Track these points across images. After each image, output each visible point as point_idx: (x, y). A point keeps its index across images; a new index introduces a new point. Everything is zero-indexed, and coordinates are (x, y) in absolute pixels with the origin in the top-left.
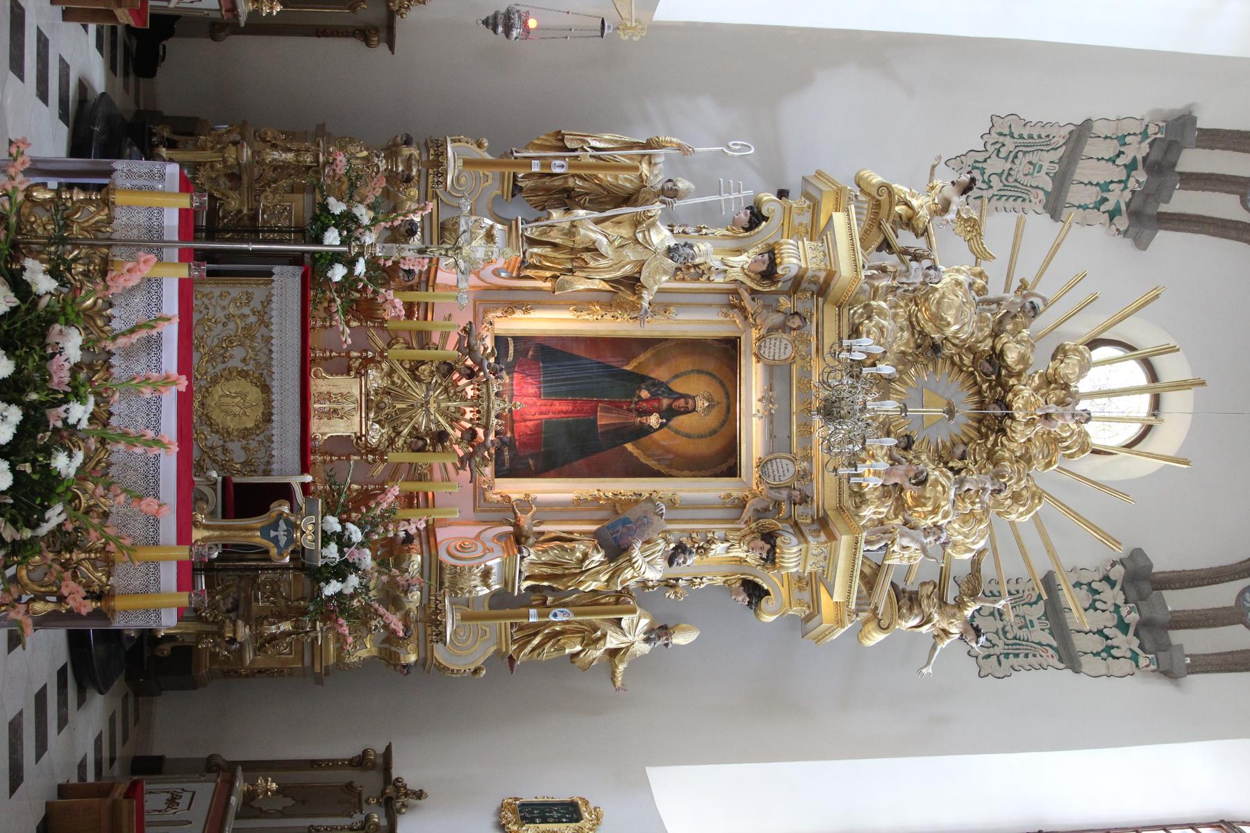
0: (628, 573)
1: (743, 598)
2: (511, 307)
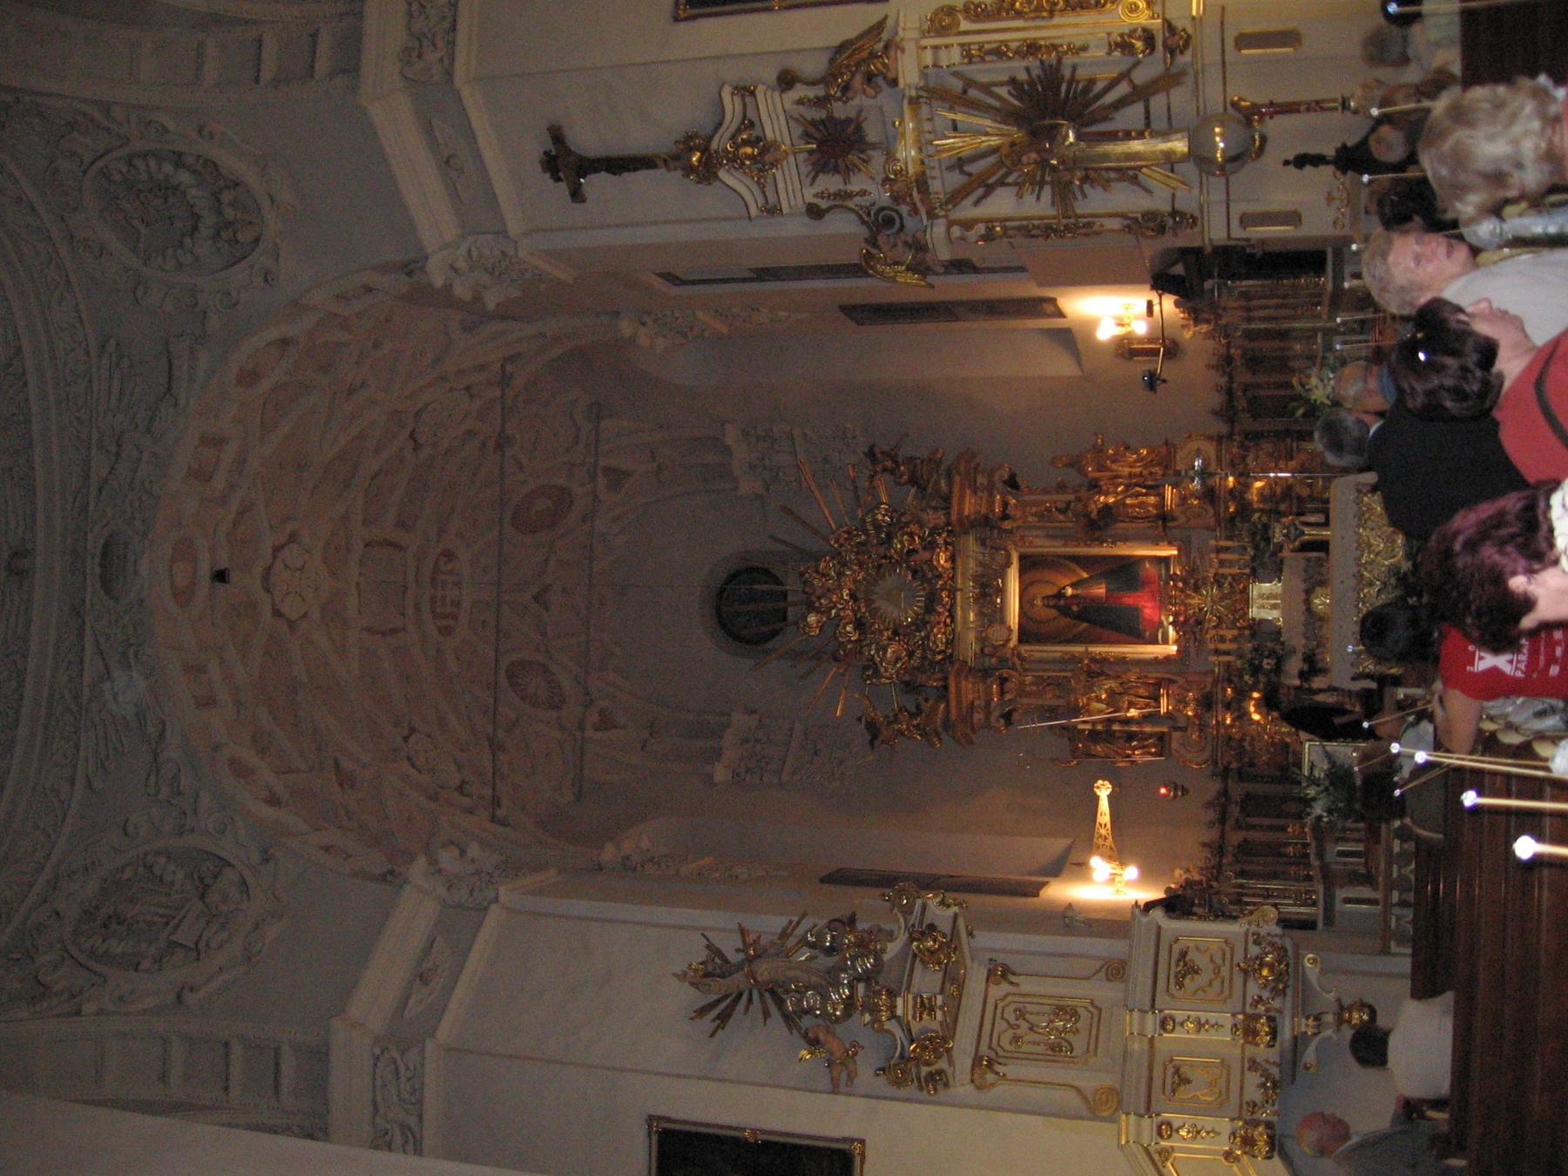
2: (1168, 659)
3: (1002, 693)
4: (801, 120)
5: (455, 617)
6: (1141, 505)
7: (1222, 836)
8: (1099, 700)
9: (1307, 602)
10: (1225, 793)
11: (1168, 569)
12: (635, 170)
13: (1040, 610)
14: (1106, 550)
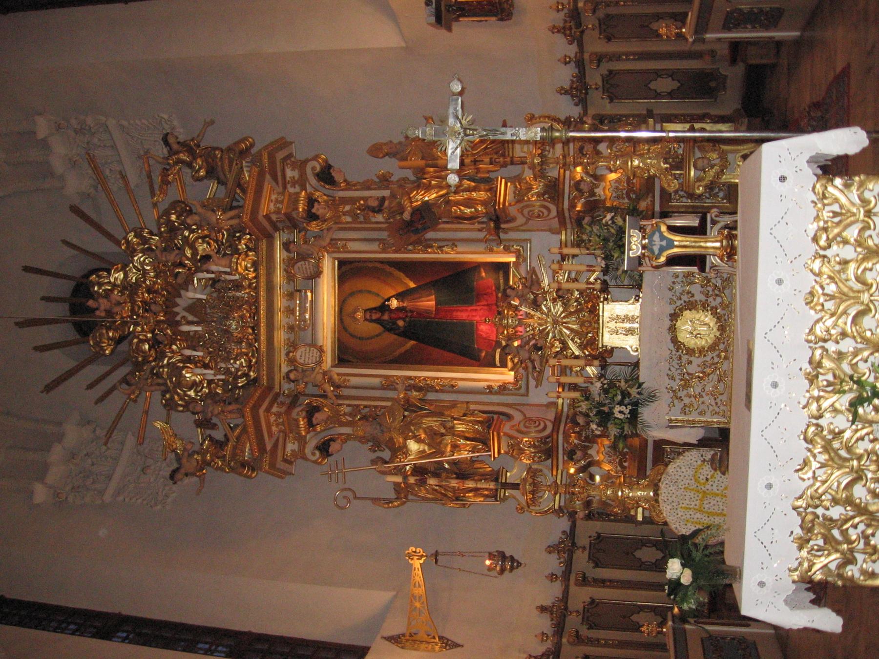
3: (311, 425)
6: (469, 203)
8: (419, 441)
9: (673, 329)
11: (507, 279)
13: (364, 327)
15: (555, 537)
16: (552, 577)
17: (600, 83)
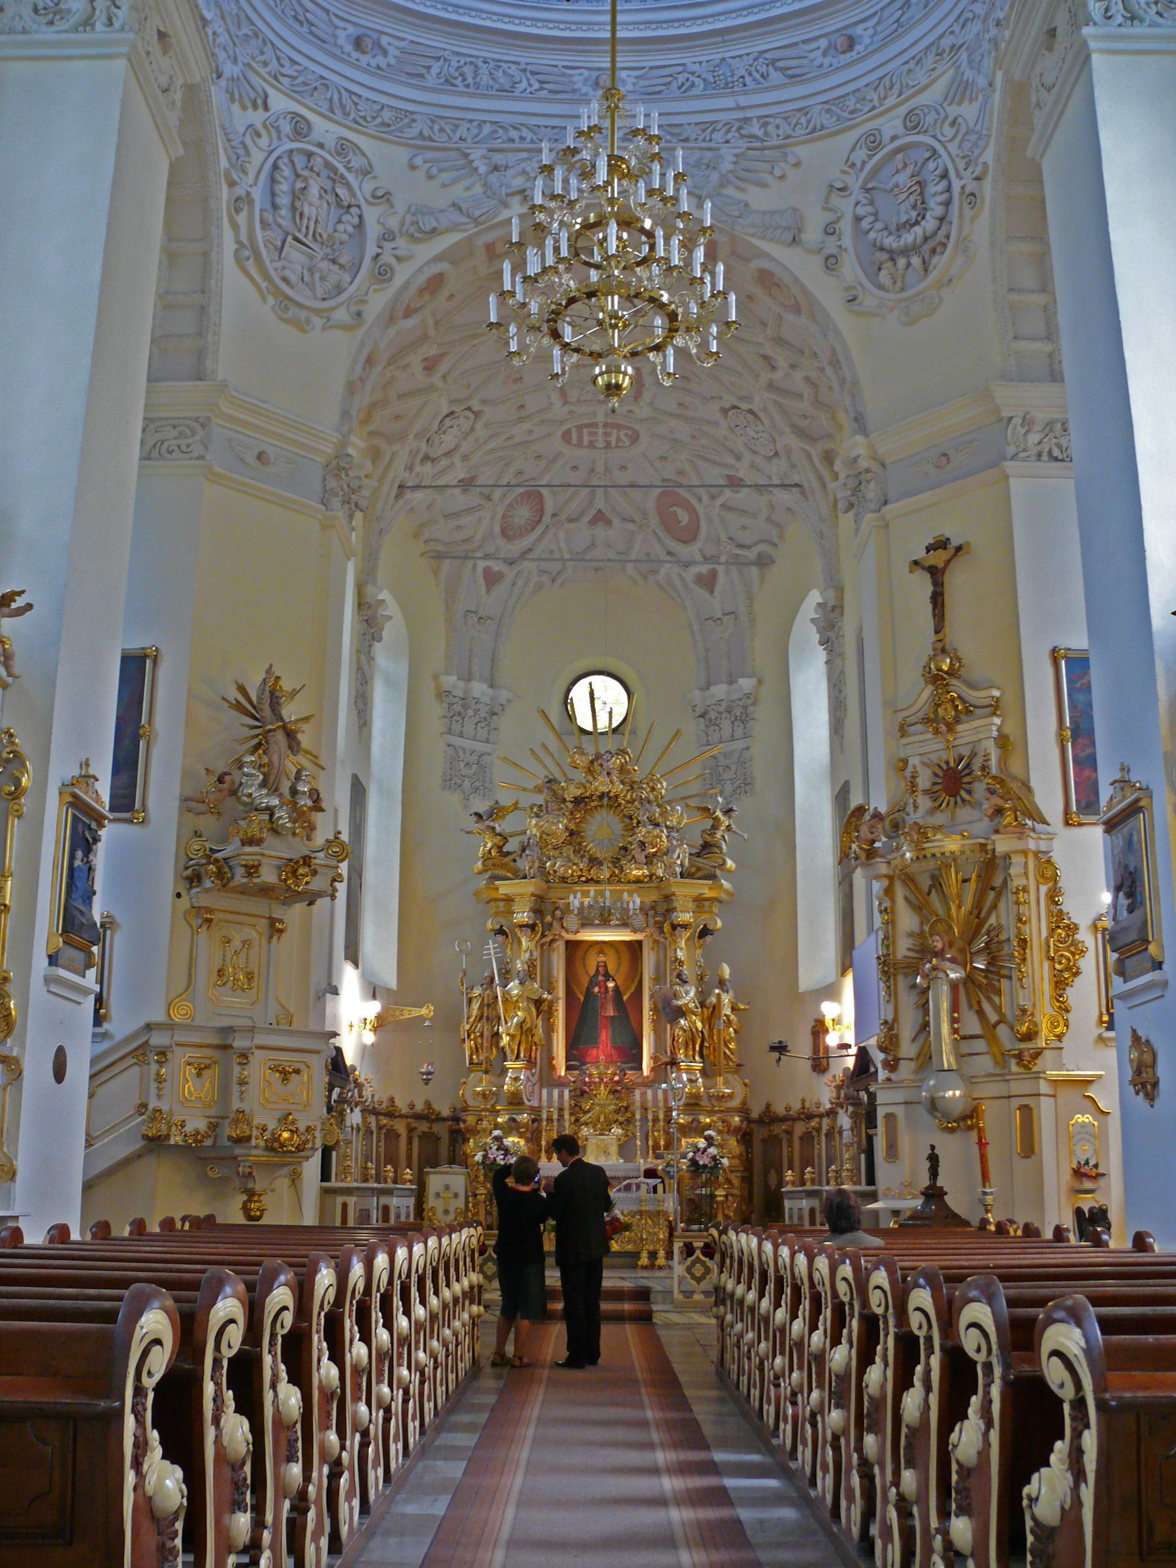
0: (692, 1005)
1: (709, 938)
2: (553, 1068)
4: (973, 755)
5: (580, 444)
7: (401, 1116)
10: (439, 1119)
12: (934, 615)
14: (647, 1013)
15: (437, 1107)
16: (412, 1106)
17: (775, 1133)
